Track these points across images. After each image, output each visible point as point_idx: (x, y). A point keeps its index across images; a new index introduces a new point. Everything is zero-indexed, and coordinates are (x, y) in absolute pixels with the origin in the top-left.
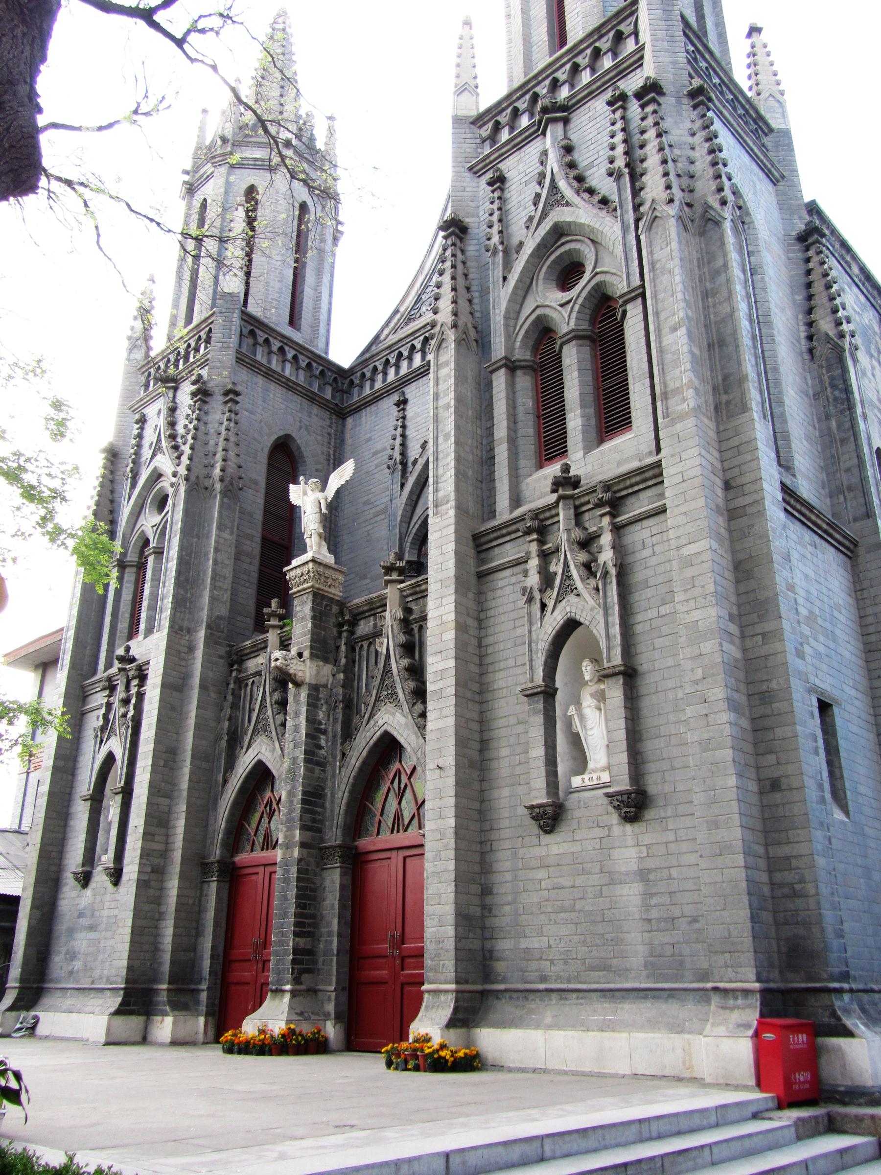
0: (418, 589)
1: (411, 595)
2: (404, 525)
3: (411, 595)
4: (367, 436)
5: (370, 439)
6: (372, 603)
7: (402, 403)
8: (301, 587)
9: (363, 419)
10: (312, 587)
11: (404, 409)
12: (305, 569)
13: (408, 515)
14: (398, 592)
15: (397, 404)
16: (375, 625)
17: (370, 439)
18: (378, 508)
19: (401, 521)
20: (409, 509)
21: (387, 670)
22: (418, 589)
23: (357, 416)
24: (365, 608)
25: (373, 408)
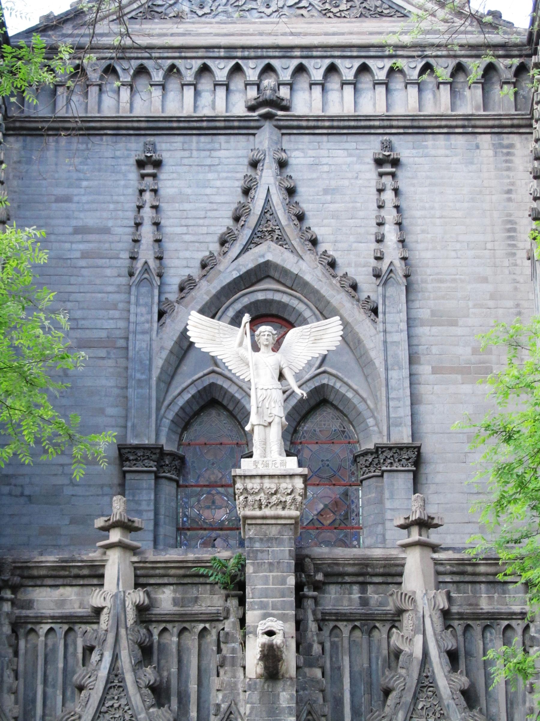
0: (469, 569)
1: (453, 573)
2: (162, 385)
3: (453, 573)
4: (60, 191)
5: (67, 199)
6: (367, 565)
7: (150, 164)
8: (267, 512)
9: (50, 154)
10: (296, 518)
11: (154, 176)
12: (286, 485)
13: (171, 370)
14: (432, 565)
15: (141, 164)
16: (364, 602)
17: (67, 199)
18: (88, 334)
19: (159, 379)
20: (174, 360)
21: (425, 684)
22: (469, 569)
23: (34, 142)
24: (350, 569)
25: (77, 143)
